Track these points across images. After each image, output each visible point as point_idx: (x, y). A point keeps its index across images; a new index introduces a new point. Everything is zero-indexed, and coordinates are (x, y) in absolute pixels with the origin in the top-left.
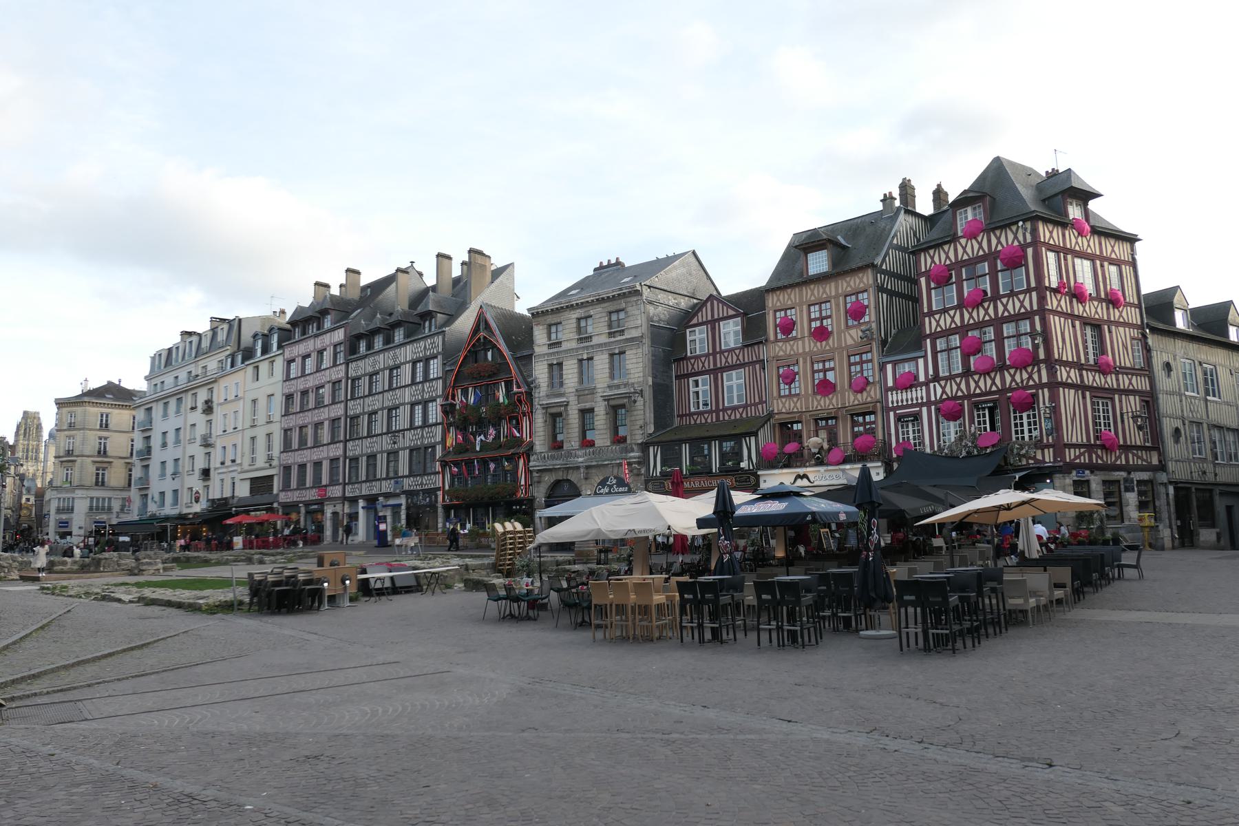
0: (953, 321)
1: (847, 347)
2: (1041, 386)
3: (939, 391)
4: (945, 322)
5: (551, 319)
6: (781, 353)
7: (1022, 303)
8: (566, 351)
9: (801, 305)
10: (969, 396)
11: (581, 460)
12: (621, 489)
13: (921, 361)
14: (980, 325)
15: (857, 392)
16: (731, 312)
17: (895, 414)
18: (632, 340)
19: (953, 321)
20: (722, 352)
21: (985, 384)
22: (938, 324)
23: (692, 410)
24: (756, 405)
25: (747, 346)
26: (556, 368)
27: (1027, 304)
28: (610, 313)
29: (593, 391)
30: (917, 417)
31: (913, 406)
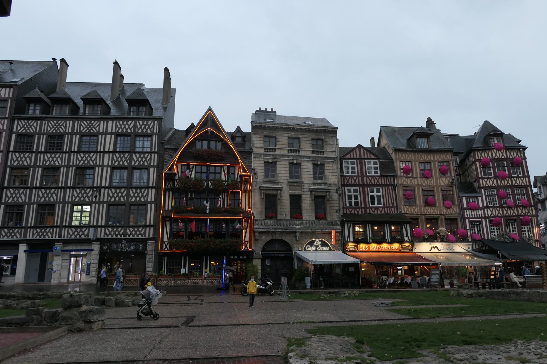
0: (493, 183)
1: (441, 186)
2: (533, 216)
3: (490, 213)
4: (490, 183)
5: (267, 133)
6: (405, 183)
7: (522, 181)
8: (279, 155)
9: (415, 161)
10: (504, 216)
11: (298, 227)
12: (324, 248)
13: (480, 199)
14: (505, 187)
15: (448, 208)
16: (372, 156)
17: (469, 221)
18: (330, 158)
19: (493, 183)
20: (367, 177)
21: (510, 212)
22: (486, 183)
23: (348, 205)
24: (390, 207)
25: (384, 176)
26: (270, 166)
27: (524, 181)
28: (313, 139)
29: (301, 185)
30: (481, 223)
31: (477, 218)
